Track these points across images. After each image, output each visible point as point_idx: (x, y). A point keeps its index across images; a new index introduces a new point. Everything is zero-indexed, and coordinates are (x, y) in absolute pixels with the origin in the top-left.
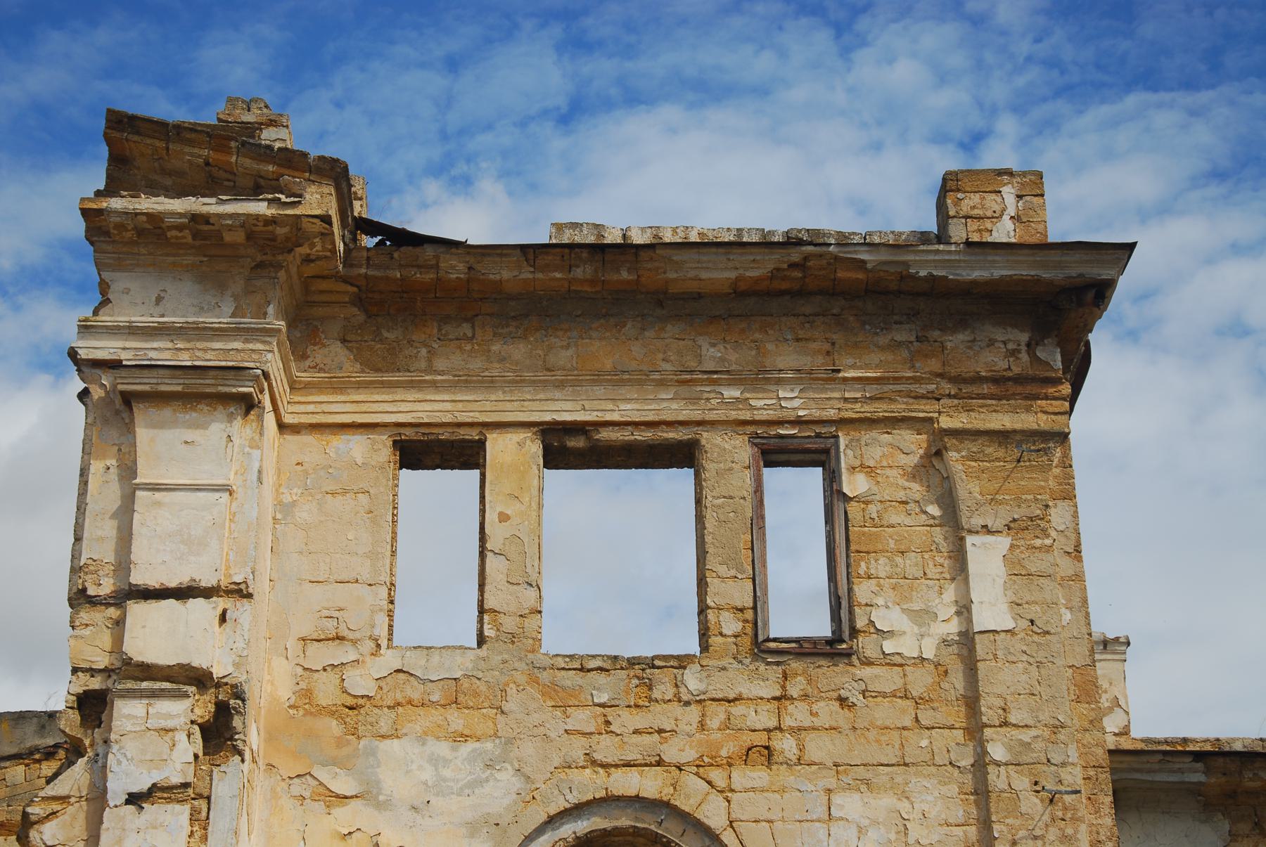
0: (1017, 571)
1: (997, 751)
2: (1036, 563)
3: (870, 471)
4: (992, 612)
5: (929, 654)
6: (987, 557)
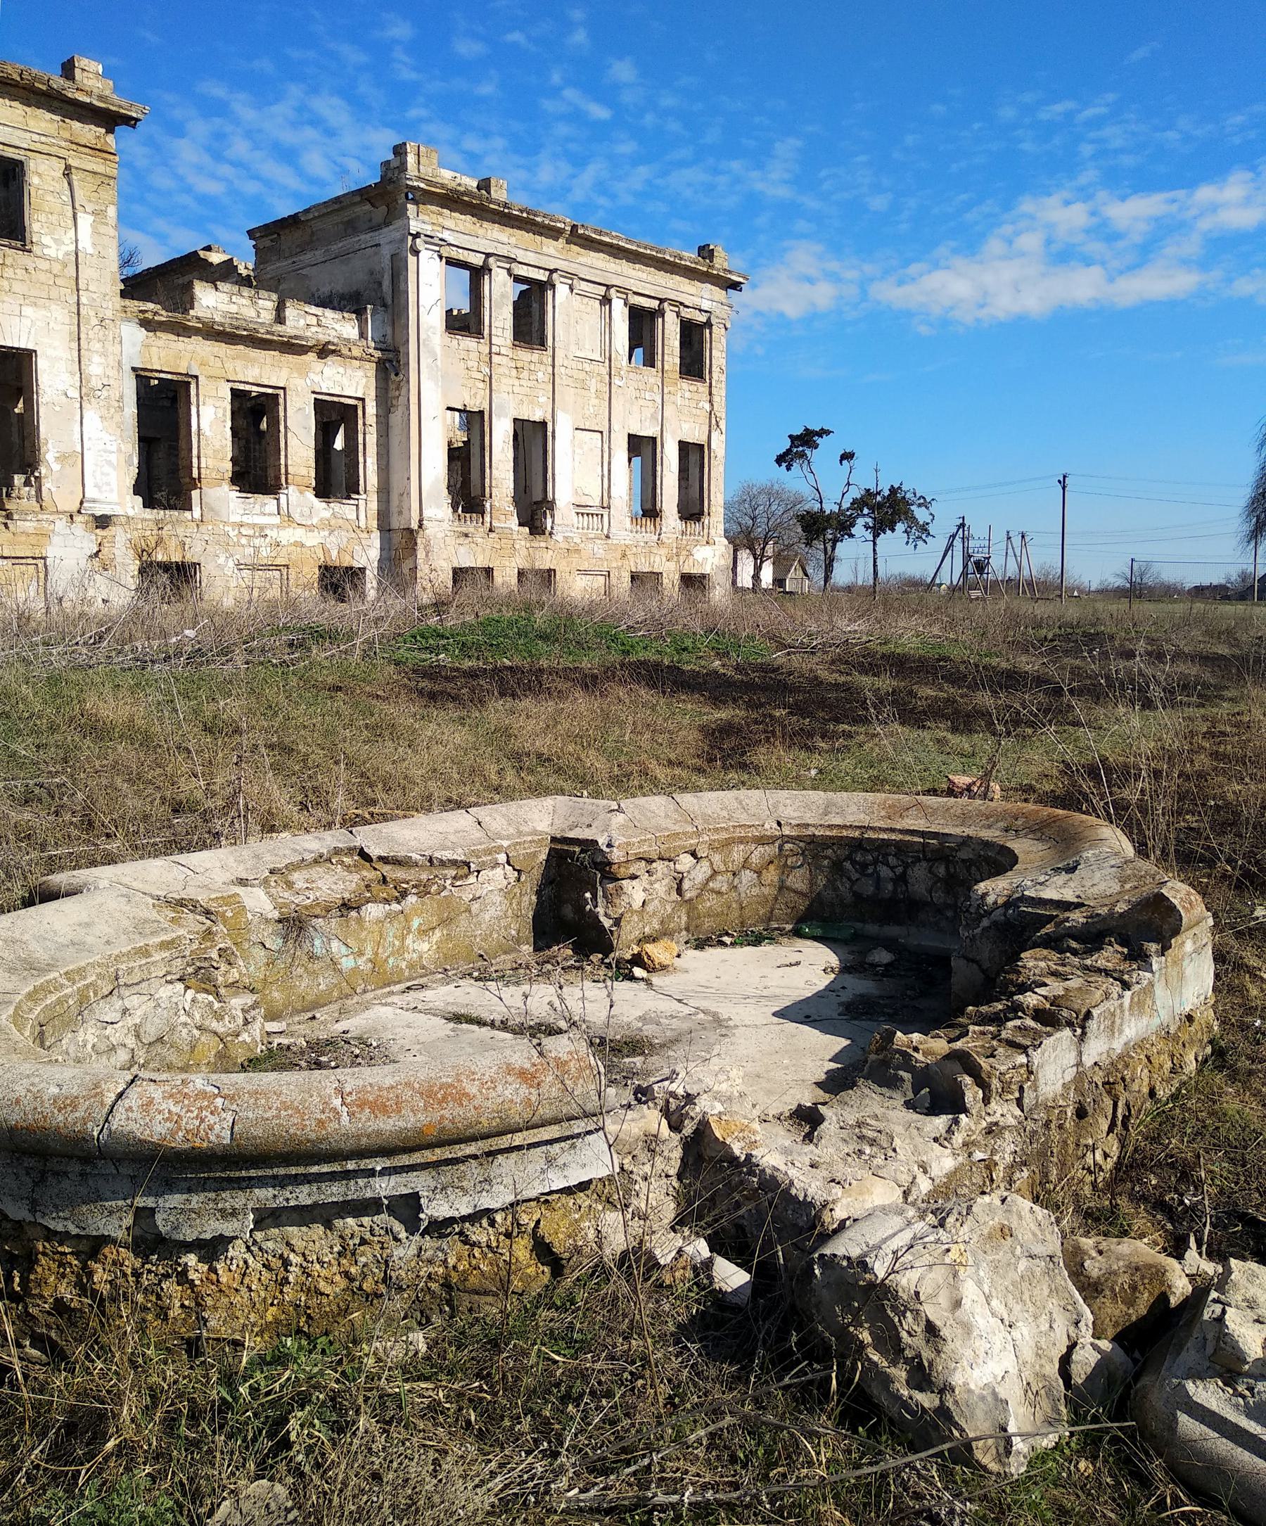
0: (95, 232)
1: (83, 300)
2: (102, 229)
3: (40, 175)
4: (86, 243)
5: (60, 257)
6: (85, 221)
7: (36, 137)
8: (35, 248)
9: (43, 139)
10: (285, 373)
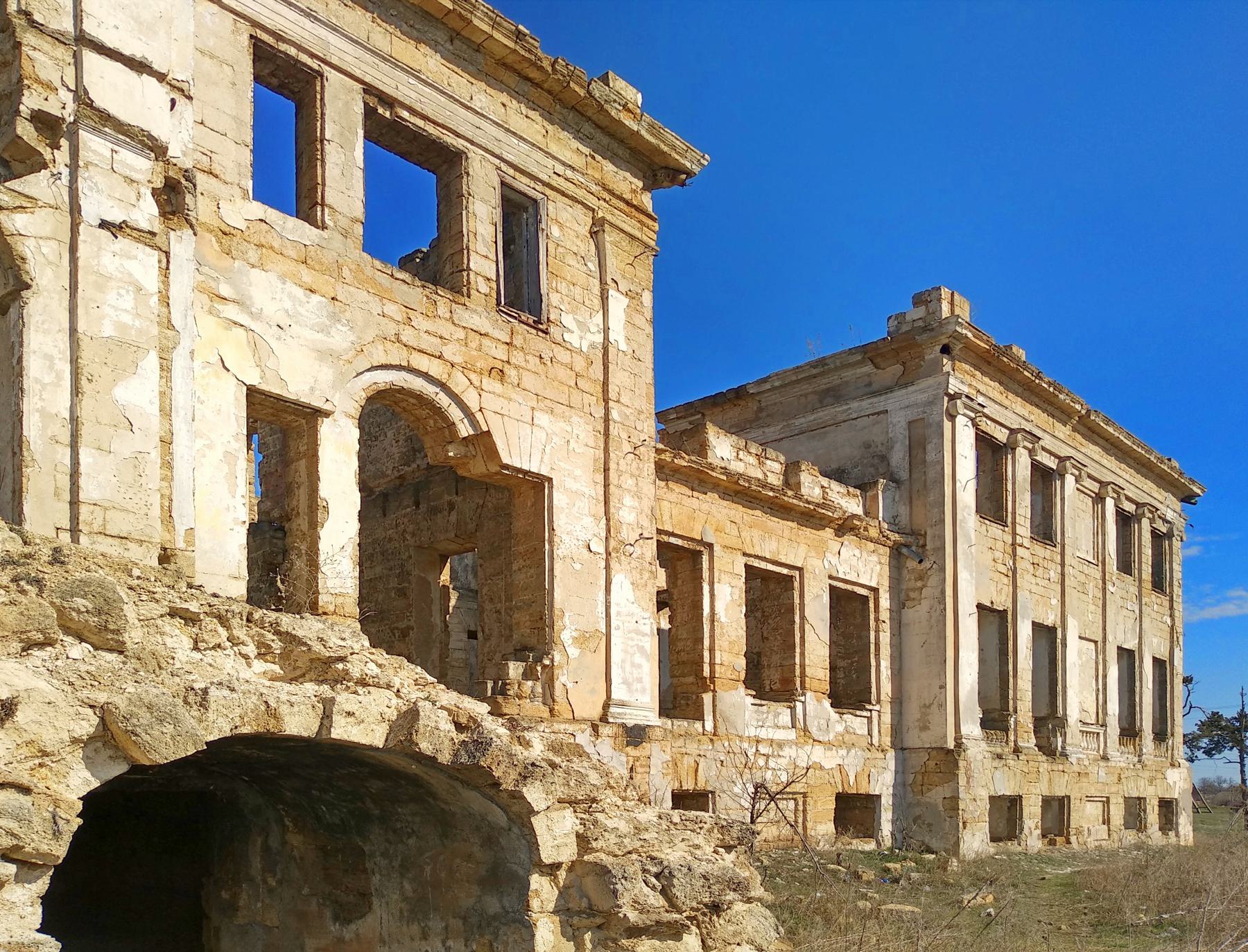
7: (560, 169)
8: (552, 330)
9: (569, 173)
10: (803, 550)
